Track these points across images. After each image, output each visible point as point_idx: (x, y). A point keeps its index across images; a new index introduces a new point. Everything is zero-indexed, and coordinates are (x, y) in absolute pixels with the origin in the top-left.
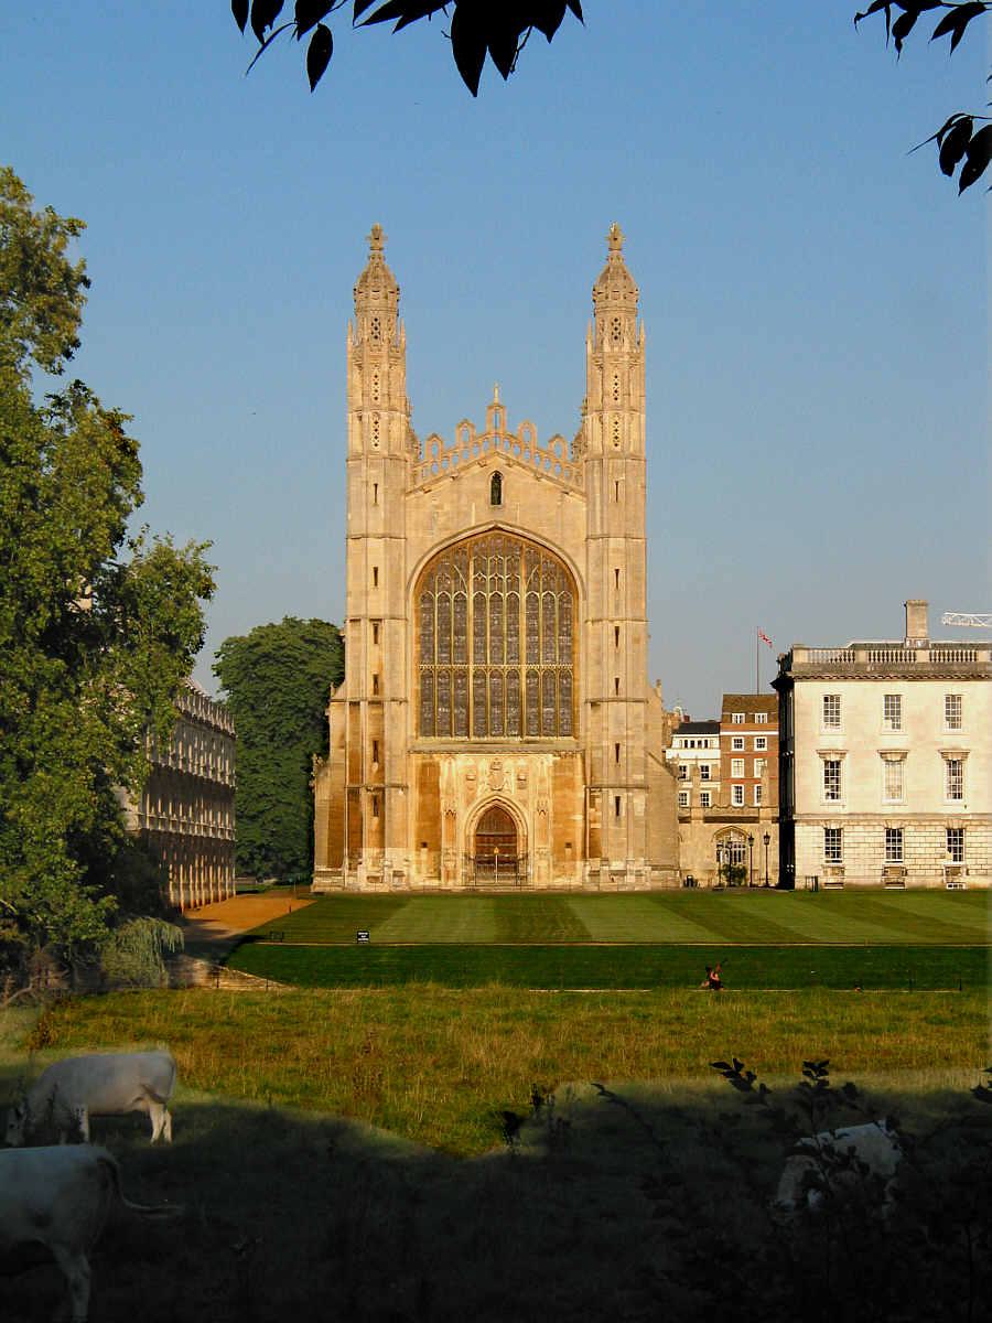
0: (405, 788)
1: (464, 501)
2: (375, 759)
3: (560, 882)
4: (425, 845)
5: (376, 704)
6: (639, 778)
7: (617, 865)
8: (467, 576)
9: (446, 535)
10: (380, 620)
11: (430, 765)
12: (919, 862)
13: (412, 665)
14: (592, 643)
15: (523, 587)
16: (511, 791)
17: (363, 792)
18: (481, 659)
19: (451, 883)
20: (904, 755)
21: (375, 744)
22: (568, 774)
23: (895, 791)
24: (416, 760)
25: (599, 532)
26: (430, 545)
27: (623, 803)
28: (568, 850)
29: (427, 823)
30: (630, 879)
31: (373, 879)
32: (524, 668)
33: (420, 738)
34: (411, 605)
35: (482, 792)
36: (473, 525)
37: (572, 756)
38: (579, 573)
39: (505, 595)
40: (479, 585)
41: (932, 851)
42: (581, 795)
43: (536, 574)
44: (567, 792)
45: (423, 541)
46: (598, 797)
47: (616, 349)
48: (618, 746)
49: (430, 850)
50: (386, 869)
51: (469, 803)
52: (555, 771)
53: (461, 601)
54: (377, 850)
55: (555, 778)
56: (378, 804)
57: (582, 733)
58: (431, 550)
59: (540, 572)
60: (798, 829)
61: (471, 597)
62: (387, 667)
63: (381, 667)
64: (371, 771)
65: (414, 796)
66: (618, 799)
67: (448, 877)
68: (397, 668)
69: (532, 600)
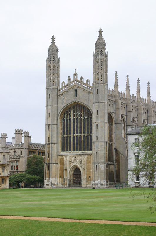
0: (56, 164)
1: (69, 96)
2: (49, 157)
3: (88, 186)
4: (61, 177)
5: (49, 144)
6: (103, 160)
7: (96, 182)
8: (71, 114)
9: (65, 105)
10: (50, 125)
13: (60, 135)
15: (82, 115)
17: (46, 165)
18: (74, 133)
19: (66, 186)
21: (49, 153)
22: (90, 160)
26: (62, 107)
27: (98, 166)
28: (90, 178)
31: (47, 185)
32: (82, 135)
35: (73, 165)
36: (71, 102)
39: (79, 118)
40: (74, 115)
42: (92, 165)
43: (85, 113)
44: (89, 164)
45: (62, 106)
47: (97, 58)
48: (97, 153)
53: (70, 120)
54: (48, 178)
55: (87, 161)
56: (49, 167)
59: (86, 112)
60: (129, 172)
61: (72, 118)
62: (51, 136)
63: (50, 136)
64: (47, 160)
65: (59, 166)
66: (97, 166)
67: (65, 185)
68: (54, 136)
69: (84, 119)
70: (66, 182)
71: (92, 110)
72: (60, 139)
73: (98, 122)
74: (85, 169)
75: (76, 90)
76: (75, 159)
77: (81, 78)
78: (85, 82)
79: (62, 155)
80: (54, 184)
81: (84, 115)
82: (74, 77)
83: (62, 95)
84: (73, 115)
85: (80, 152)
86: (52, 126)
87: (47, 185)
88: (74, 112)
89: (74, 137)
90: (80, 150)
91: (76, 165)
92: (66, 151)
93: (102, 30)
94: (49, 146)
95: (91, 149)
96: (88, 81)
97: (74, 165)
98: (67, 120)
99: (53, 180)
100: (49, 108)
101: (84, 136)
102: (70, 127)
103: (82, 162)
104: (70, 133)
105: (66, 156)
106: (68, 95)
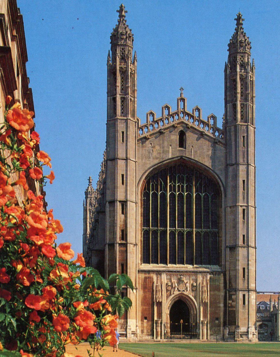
4: (146, 318)
9: (156, 161)
11: (148, 278)
14: (230, 217)
18: (173, 225)
19: (159, 338)
21: (122, 265)
25: (234, 162)
26: (148, 166)
27: (246, 297)
28: (217, 322)
29: (147, 307)
30: (250, 336)
31: (122, 335)
33: (143, 264)
34: (140, 197)
36: (170, 156)
37: (219, 275)
38: (222, 183)
40: (173, 188)
44: (217, 292)
46: (234, 295)
49: (148, 321)
50: (128, 330)
51: (167, 297)
52: (210, 282)
53: (164, 196)
57: (223, 263)
58: (149, 168)
66: (244, 296)
69: (198, 197)
70: (159, 329)
71: (223, 179)
73: (246, 206)
74: (207, 303)
79: (149, 272)
83: (149, 139)
84: (170, 186)
85: (190, 267)
87: (122, 335)
91: (183, 292)
92: (152, 263)
93: (242, 18)
94: (123, 249)
97: (177, 293)
98: (155, 195)
105: (159, 273)
106: (163, 140)
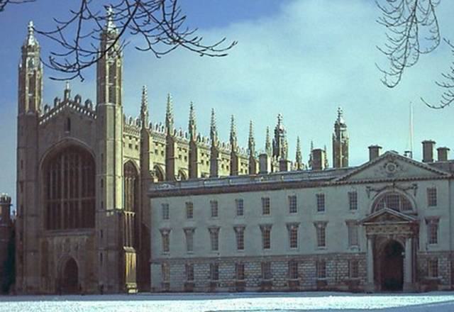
0: (35, 251)
7: (101, 283)
12: (200, 280)
15: (80, 165)
16: (72, 254)
18: (66, 197)
20: (193, 231)
21: (21, 234)
23: (189, 247)
24: (41, 240)
27: (104, 255)
32: (80, 199)
39: (74, 169)
40: (66, 165)
41: (204, 275)
45: (45, 149)
48: (102, 231)
53: (59, 173)
60: (152, 266)
66: (101, 254)
69: (83, 170)
72: (42, 208)
75: (69, 120)
76: (68, 241)
77: (77, 97)
78: (83, 104)
80: (31, 288)
81: (83, 166)
82: (65, 96)
86: (26, 185)
88: (66, 158)
89: (65, 203)
90: (77, 227)
95: (92, 224)
96: (87, 102)
99: (30, 280)
100: (21, 150)
101: (83, 203)
102: (59, 184)
103: (79, 248)
104: (60, 197)
